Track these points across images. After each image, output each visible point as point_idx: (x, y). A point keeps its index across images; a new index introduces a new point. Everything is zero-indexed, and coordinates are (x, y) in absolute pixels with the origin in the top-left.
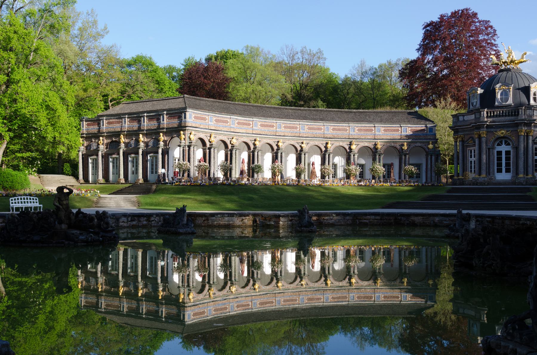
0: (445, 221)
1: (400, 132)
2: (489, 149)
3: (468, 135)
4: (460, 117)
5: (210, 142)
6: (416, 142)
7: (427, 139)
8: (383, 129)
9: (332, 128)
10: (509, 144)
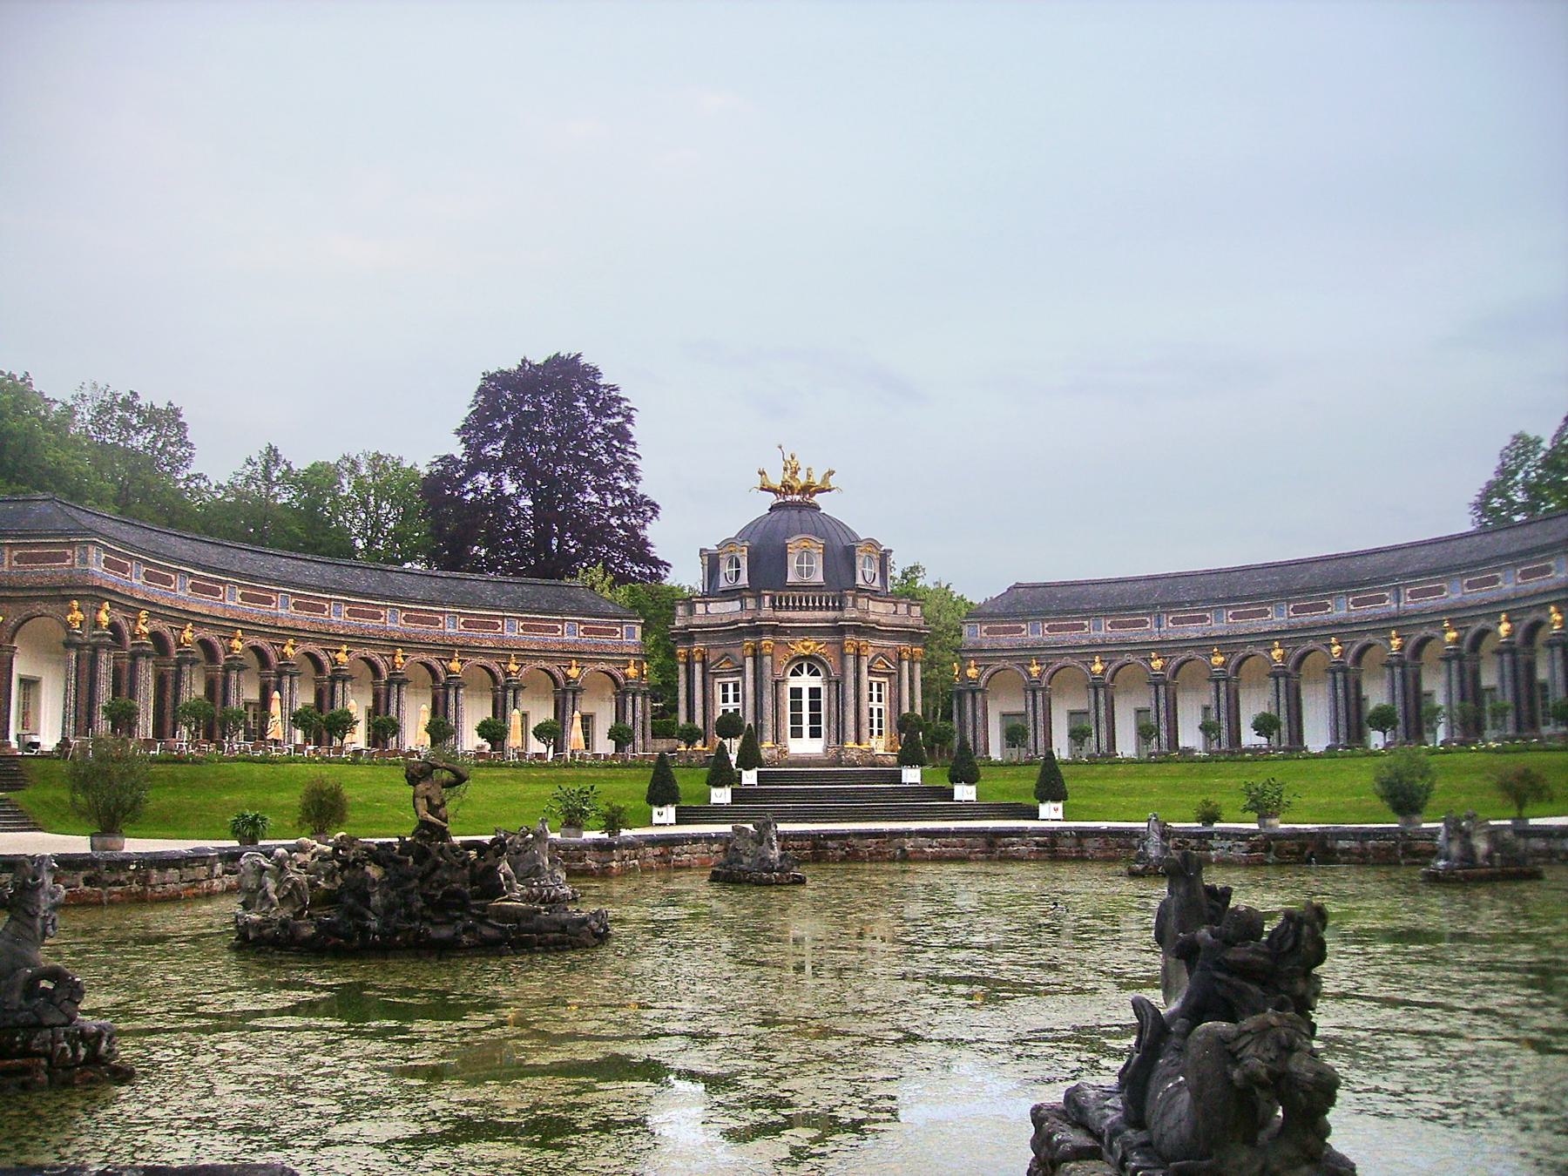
0: (930, 846)
1: (560, 633)
2: (777, 682)
3: (719, 647)
4: (697, 605)
5: (134, 637)
6: (597, 661)
7: (624, 655)
8: (522, 624)
9: (404, 615)
10: (816, 674)
